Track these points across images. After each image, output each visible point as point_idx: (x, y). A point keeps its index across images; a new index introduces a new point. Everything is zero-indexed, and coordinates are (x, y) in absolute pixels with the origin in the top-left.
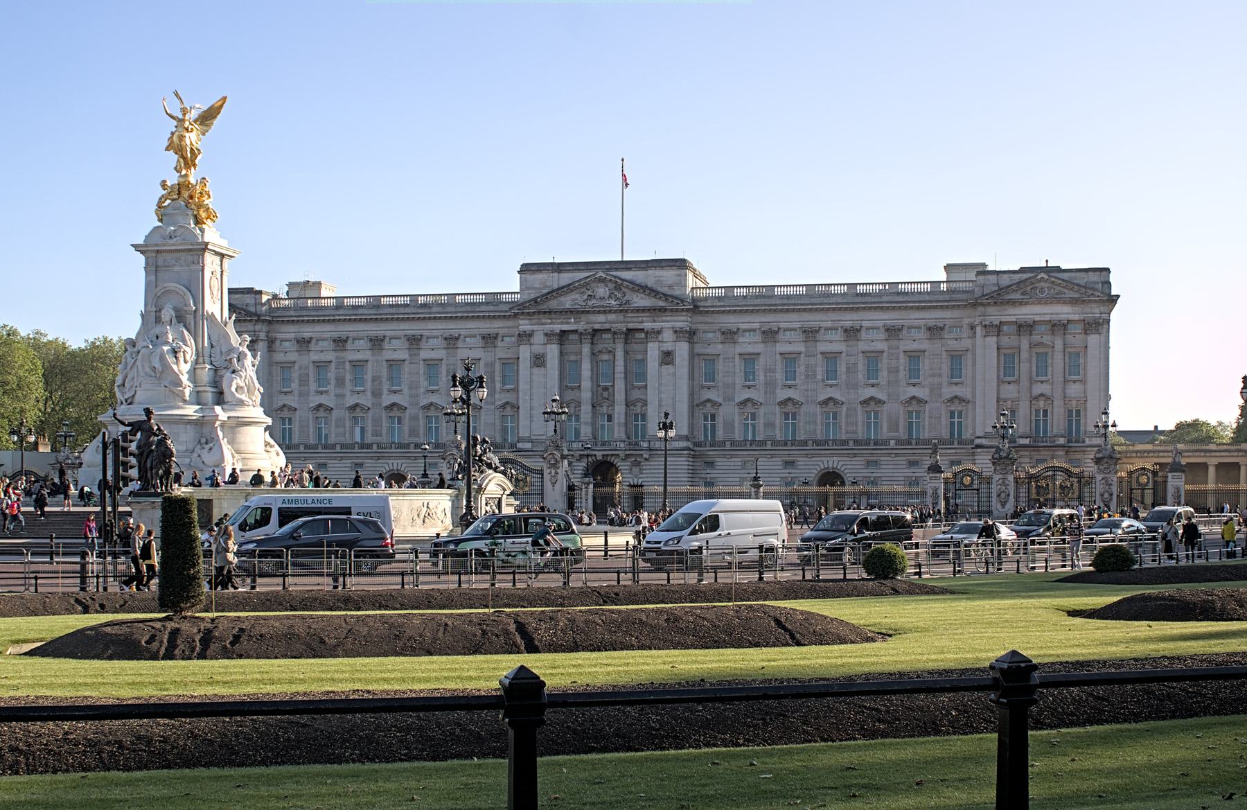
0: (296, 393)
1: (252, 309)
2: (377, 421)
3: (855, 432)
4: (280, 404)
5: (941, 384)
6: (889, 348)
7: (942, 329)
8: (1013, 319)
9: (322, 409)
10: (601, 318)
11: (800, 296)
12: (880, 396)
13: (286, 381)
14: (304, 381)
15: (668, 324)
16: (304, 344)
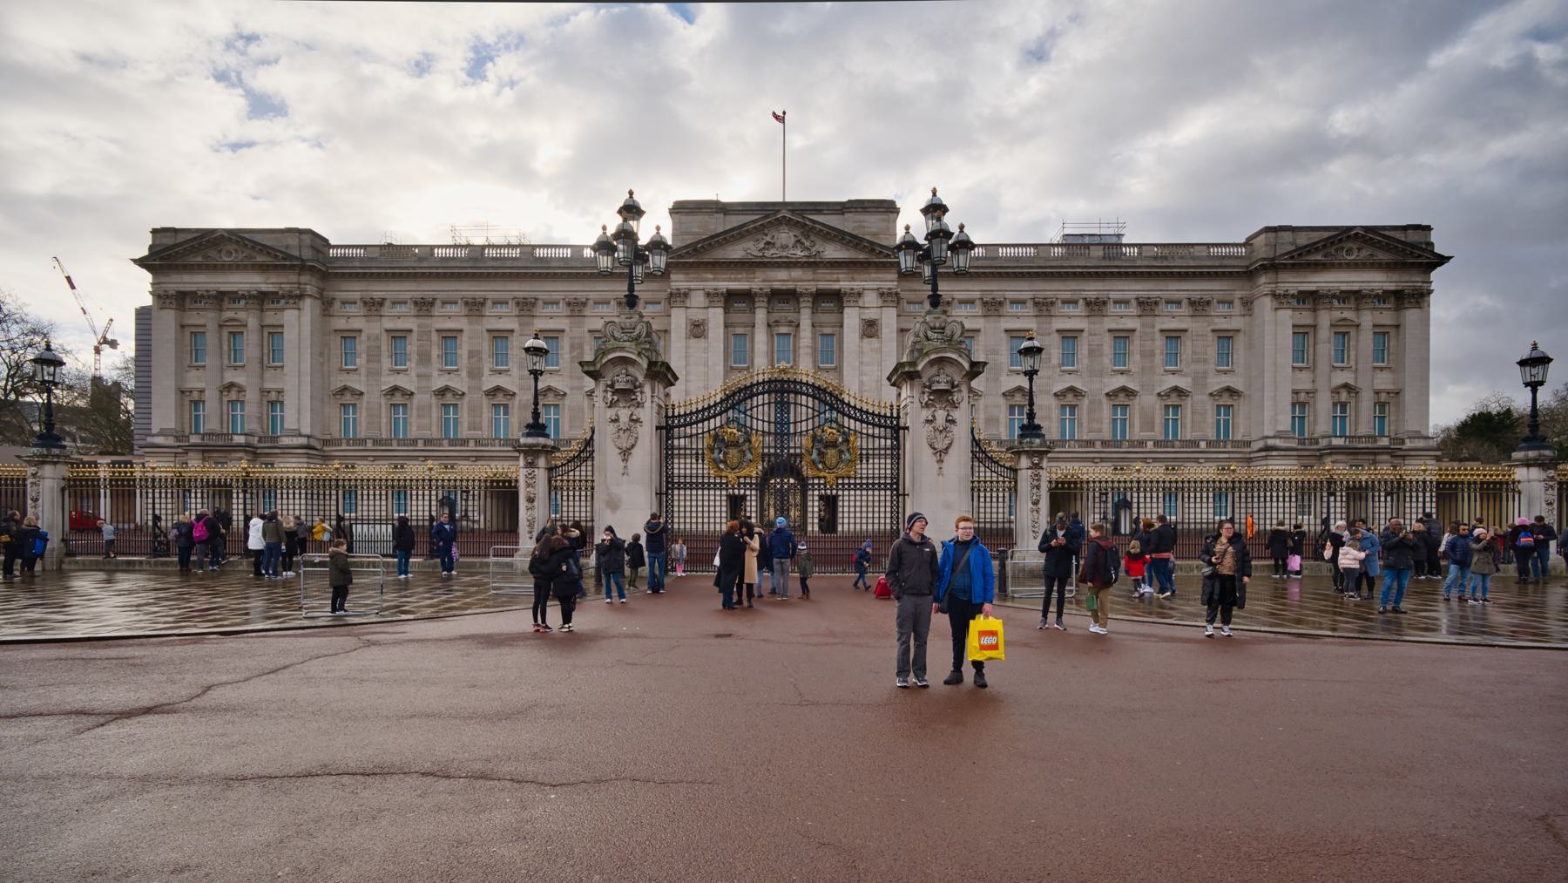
0: (363, 371)
1: (296, 253)
2: (475, 410)
3: (1100, 431)
4: (341, 385)
5: (1205, 372)
6: (1143, 325)
7: (1208, 303)
8: (1312, 287)
9: (398, 395)
10: (782, 274)
11: (1029, 258)
12: (1131, 386)
13: (349, 355)
14: (374, 356)
15: (871, 284)
16: (374, 306)
